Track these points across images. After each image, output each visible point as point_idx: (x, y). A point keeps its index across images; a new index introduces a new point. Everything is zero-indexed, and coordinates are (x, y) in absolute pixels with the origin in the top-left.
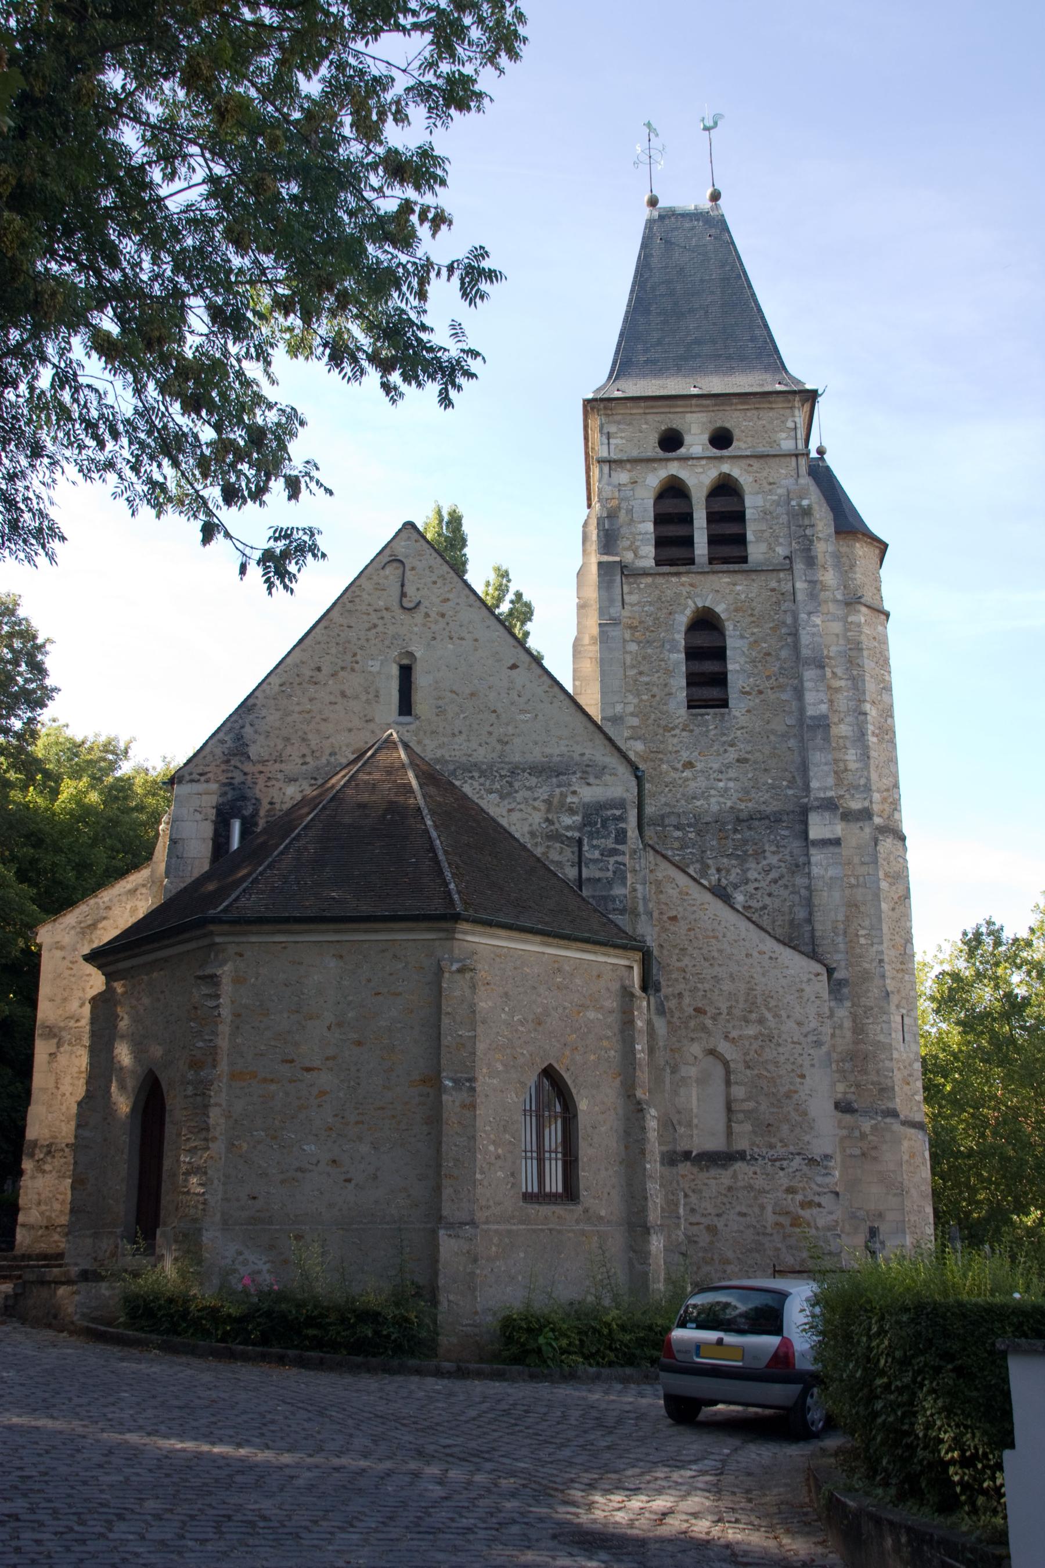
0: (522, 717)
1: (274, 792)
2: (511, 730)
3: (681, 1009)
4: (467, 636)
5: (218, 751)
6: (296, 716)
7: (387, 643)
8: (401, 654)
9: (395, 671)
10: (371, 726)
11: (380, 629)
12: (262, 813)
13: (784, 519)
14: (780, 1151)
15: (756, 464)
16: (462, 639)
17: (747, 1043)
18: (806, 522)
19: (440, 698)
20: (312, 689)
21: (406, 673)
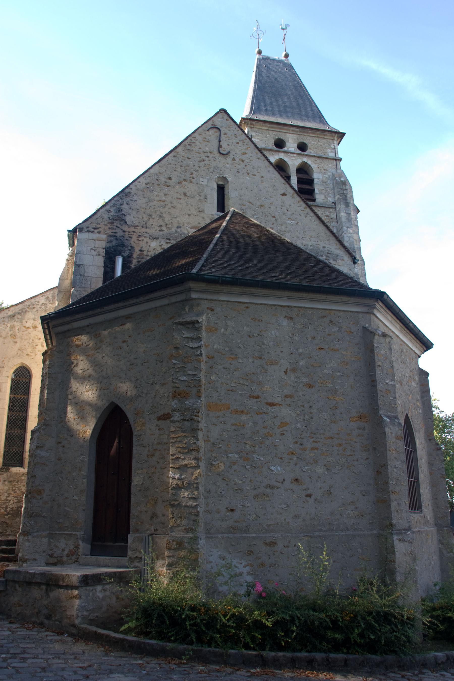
1: (143, 244)
2: (283, 228)
4: (257, 174)
5: (106, 216)
6: (155, 203)
8: (219, 177)
11: (207, 162)
12: (135, 256)
13: (331, 186)
15: (319, 161)
16: (254, 175)
18: (344, 188)
19: (242, 205)
20: (166, 189)
21: (221, 190)
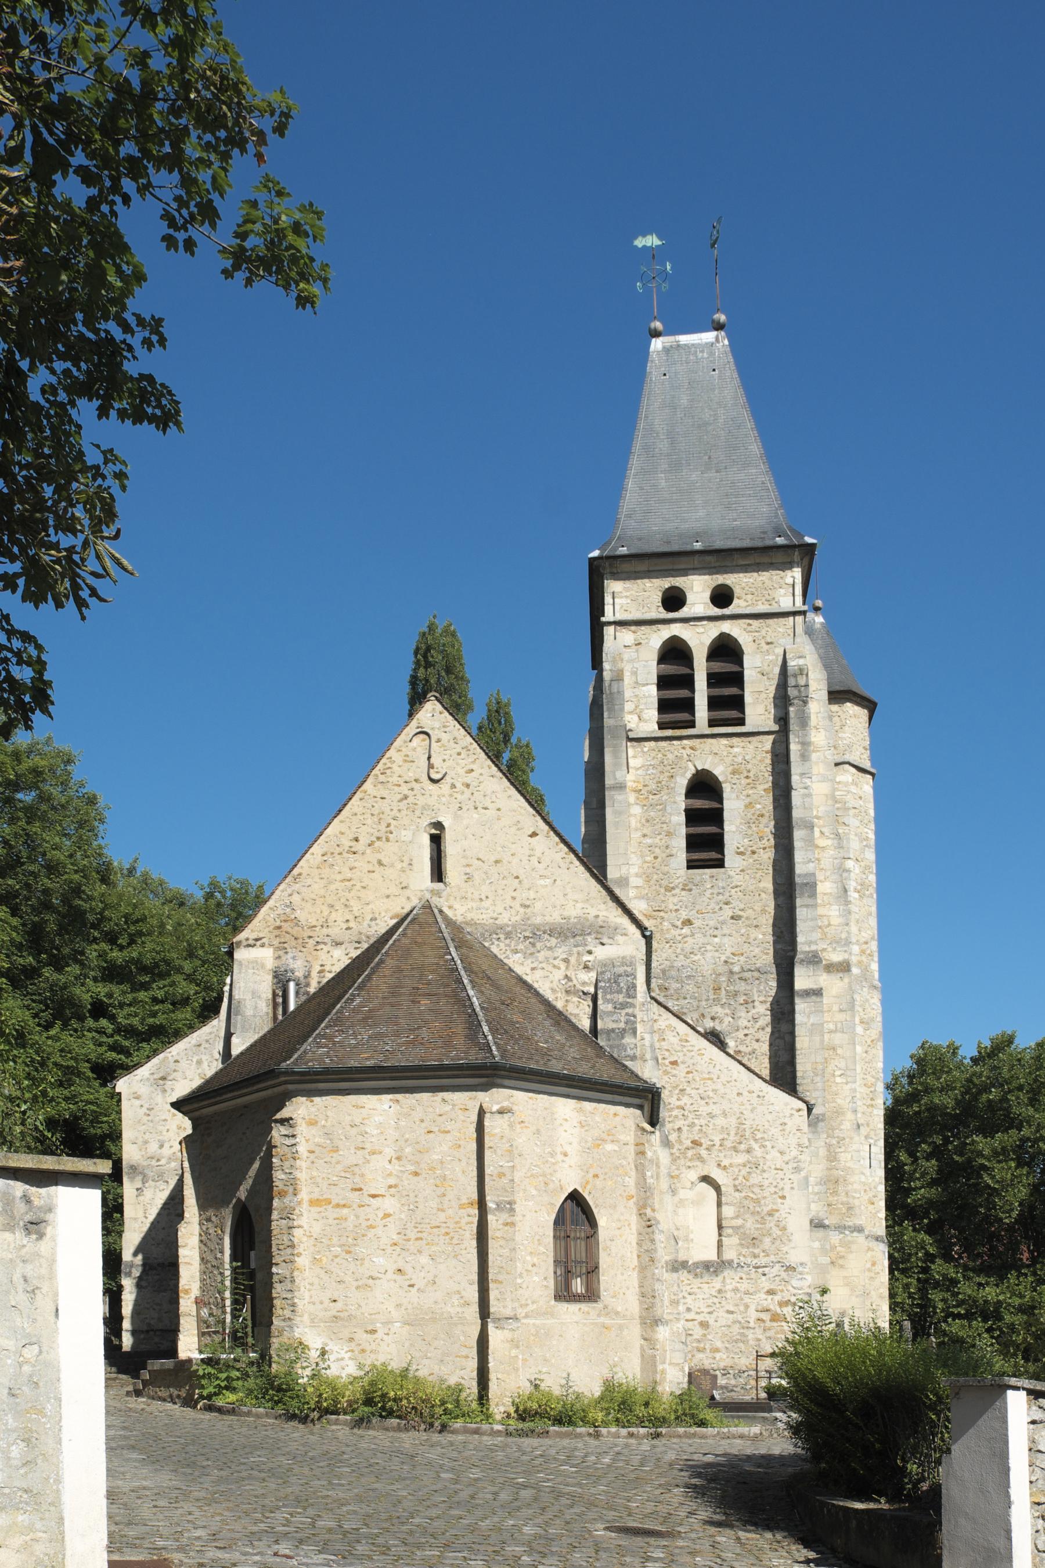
0: (542, 882)
2: (532, 894)
3: (680, 1142)
7: (418, 813)
9: (426, 840)
10: (407, 892)
14: (763, 1260)
17: (736, 1170)
19: (468, 865)
21: (436, 840)
